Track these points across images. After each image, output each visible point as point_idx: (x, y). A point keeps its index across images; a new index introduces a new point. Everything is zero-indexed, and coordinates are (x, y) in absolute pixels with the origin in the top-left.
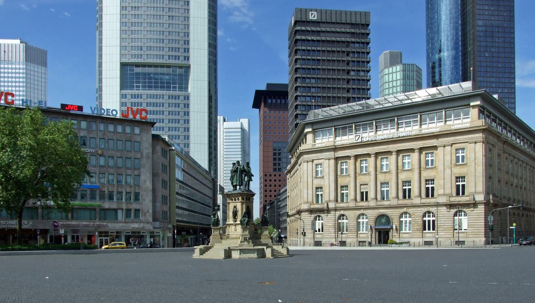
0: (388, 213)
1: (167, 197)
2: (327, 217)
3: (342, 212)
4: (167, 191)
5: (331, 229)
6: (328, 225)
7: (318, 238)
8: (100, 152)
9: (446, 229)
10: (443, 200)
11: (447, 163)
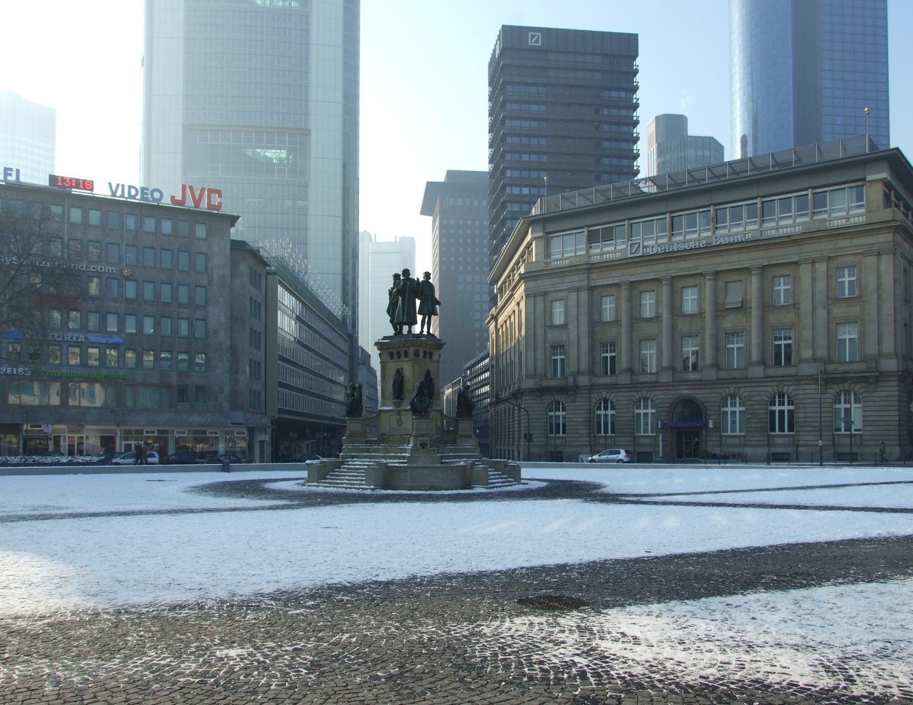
0: (697, 396)
1: (259, 363)
2: (573, 404)
3: (604, 394)
4: (259, 353)
5: (582, 427)
8: (126, 272)
10: (807, 369)
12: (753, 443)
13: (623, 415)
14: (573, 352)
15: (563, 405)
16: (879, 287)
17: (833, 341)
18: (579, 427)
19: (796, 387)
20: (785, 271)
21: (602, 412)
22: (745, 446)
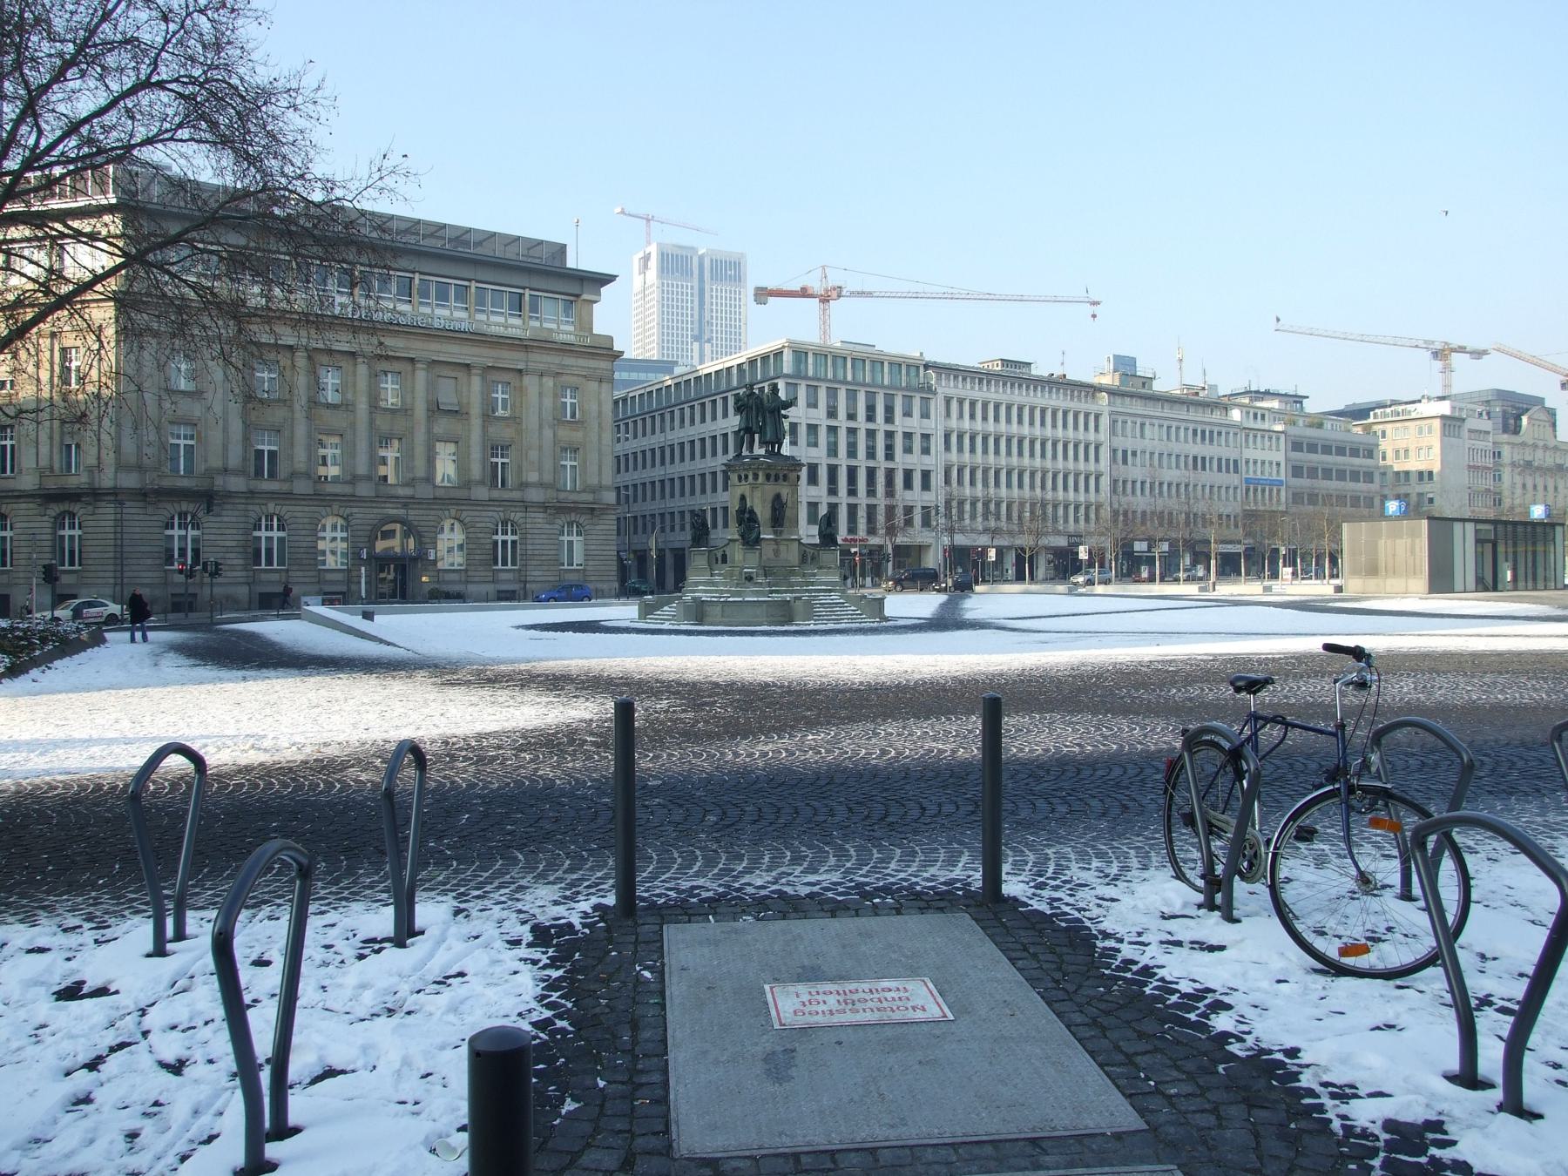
2: (218, 519)
3: (271, 507)
6: (221, 543)
7: (69, 585)
10: (534, 495)
12: (477, 579)
13: (302, 538)
14: (216, 437)
16: (600, 413)
17: (558, 469)
18: (228, 556)
20: (507, 377)
21: (263, 534)
22: (467, 582)
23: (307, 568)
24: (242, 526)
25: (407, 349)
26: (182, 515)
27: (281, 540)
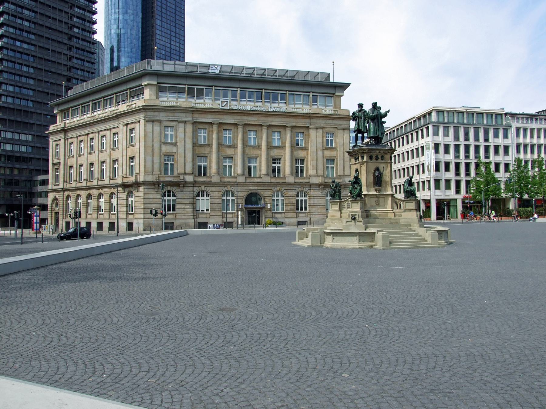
0: (260, 191)
2: (182, 193)
3: (203, 188)
5: (188, 207)
6: (183, 202)
9: (319, 209)
11: (320, 145)
13: (215, 200)
14: (181, 161)
15: (173, 193)
18: (186, 207)
19: (309, 189)
20: (302, 130)
23: (218, 212)
24: (191, 195)
25: (258, 121)
26: (169, 192)
27: (174, 200)
